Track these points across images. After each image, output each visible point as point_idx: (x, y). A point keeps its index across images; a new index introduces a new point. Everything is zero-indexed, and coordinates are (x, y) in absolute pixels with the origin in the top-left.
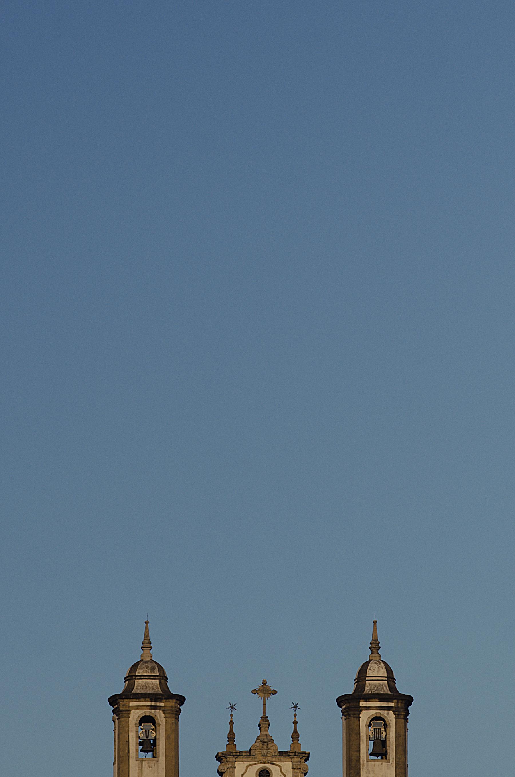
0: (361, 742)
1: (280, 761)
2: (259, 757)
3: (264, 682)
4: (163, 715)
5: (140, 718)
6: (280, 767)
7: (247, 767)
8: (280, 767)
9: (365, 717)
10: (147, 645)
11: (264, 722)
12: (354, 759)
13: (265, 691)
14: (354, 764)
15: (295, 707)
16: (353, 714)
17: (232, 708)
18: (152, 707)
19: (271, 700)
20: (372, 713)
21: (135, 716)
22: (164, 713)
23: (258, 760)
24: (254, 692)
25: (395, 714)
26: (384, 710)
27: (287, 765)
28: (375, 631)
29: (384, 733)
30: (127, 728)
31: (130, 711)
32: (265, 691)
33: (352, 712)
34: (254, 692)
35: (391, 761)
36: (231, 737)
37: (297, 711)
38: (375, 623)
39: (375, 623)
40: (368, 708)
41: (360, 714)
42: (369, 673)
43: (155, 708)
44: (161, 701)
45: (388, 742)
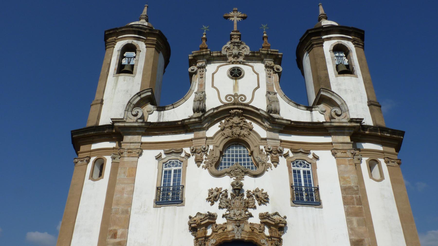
0: (327, 64)
2: (231, 59)
4: (145, 46)
5: (123, 46)
6: (252, 67)
7: (218, 67)
8: (252, 67)
9: (328, 46)
16: (316, 44)
20: (334, 42)
21: (119, 45)
22: (146, 44)
23: (229, 61)
25: (354, 44)
26: (345, 40)
27: (260, 67)
29: (347, 60)
30: (110, 55)
31: (116, 42)
33: (315, 43)
35: (359, 76)
41: (322, 43)
43: (138, 39)
45: (352, 66)
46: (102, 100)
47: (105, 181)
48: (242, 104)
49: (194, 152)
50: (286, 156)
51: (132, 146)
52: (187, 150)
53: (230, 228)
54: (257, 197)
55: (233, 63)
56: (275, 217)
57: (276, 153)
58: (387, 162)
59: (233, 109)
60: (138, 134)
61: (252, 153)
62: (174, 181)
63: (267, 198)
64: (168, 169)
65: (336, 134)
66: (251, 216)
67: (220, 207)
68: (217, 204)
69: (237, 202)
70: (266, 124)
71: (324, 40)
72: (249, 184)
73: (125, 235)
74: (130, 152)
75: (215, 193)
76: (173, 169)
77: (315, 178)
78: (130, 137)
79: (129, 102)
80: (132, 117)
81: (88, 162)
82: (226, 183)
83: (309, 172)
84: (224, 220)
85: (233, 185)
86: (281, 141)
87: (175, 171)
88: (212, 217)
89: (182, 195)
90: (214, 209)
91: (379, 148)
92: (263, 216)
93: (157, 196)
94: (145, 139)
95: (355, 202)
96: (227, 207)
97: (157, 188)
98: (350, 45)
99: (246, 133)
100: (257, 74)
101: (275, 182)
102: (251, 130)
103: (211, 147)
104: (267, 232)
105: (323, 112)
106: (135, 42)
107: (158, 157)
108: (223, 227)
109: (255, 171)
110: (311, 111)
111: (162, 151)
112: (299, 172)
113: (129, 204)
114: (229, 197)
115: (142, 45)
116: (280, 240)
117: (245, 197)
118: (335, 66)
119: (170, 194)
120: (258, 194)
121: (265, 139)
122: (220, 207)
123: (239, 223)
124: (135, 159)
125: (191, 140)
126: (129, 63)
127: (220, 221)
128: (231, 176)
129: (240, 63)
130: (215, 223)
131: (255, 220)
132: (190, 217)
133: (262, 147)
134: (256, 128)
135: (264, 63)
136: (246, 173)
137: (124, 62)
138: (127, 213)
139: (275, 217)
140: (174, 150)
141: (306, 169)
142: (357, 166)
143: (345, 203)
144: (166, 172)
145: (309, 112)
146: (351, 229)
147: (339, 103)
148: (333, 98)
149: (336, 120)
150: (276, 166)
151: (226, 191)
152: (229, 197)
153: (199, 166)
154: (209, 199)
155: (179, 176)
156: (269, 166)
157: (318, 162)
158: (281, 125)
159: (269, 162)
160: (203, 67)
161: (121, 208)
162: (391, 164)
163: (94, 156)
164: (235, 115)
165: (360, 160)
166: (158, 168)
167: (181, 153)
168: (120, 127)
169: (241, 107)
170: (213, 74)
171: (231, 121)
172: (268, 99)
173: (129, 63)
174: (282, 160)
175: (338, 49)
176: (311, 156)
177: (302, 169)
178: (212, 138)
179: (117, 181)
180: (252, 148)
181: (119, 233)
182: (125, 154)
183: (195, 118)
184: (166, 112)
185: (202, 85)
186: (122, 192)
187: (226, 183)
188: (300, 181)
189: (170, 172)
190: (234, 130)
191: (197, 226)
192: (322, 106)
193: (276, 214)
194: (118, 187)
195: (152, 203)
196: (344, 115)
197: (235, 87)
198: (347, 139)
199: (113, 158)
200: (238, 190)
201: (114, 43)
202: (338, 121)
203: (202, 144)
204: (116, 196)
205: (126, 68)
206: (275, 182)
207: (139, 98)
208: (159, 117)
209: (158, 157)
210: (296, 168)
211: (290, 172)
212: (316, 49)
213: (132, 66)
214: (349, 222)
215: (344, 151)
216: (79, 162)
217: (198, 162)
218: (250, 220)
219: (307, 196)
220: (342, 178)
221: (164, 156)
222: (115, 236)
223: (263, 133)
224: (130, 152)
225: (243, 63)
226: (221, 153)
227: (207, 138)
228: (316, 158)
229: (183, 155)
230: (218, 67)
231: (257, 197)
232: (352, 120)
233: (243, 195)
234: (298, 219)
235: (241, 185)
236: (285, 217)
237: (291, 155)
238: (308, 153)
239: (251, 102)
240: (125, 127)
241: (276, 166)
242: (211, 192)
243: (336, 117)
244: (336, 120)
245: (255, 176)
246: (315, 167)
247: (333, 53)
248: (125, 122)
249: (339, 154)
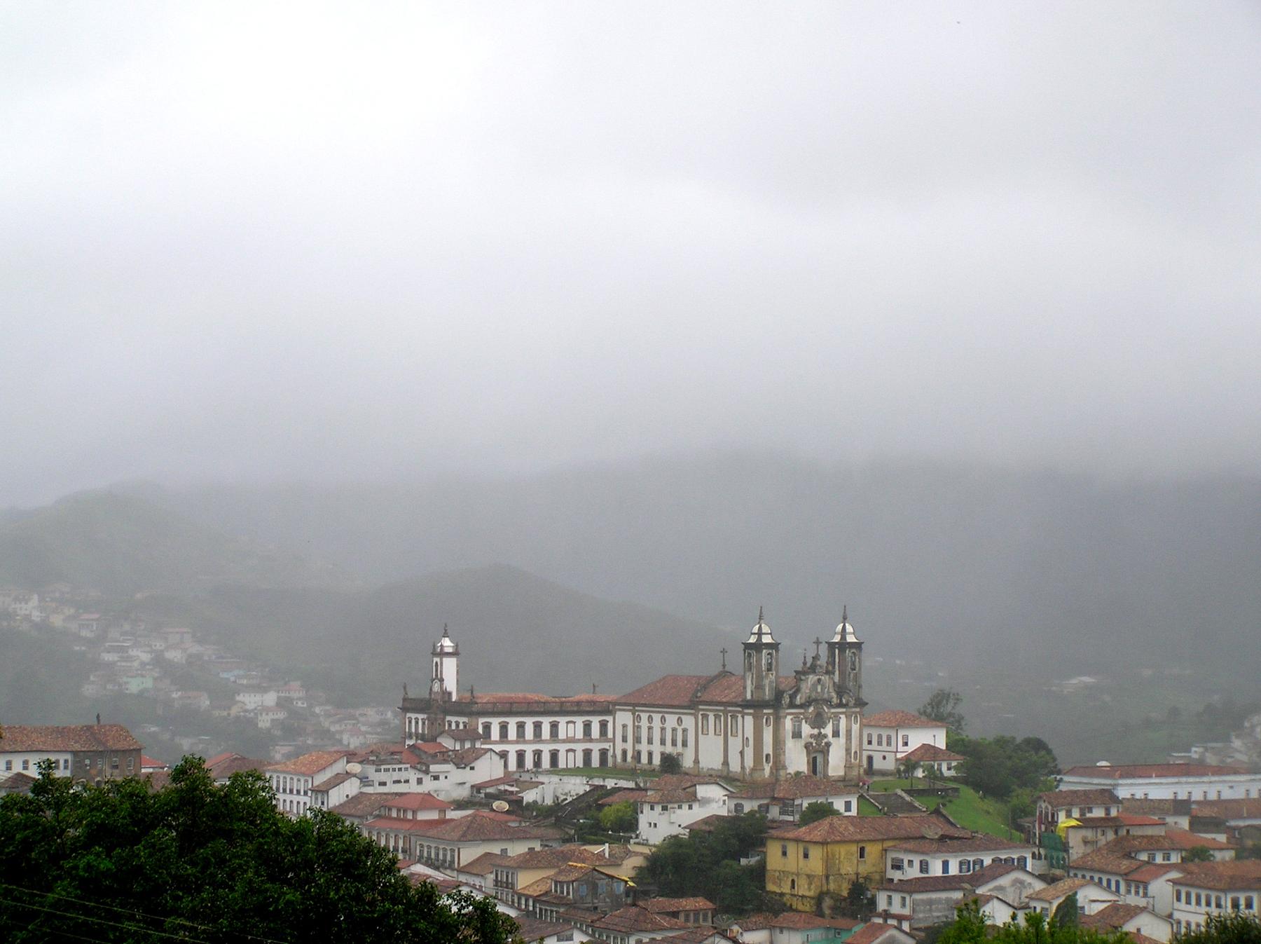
82: (816, 731)
101: (828, 730)
119: (797, 735)
140: (796, 716)
187: (816, 731)
191: (807, 746)
206: (828, 730)
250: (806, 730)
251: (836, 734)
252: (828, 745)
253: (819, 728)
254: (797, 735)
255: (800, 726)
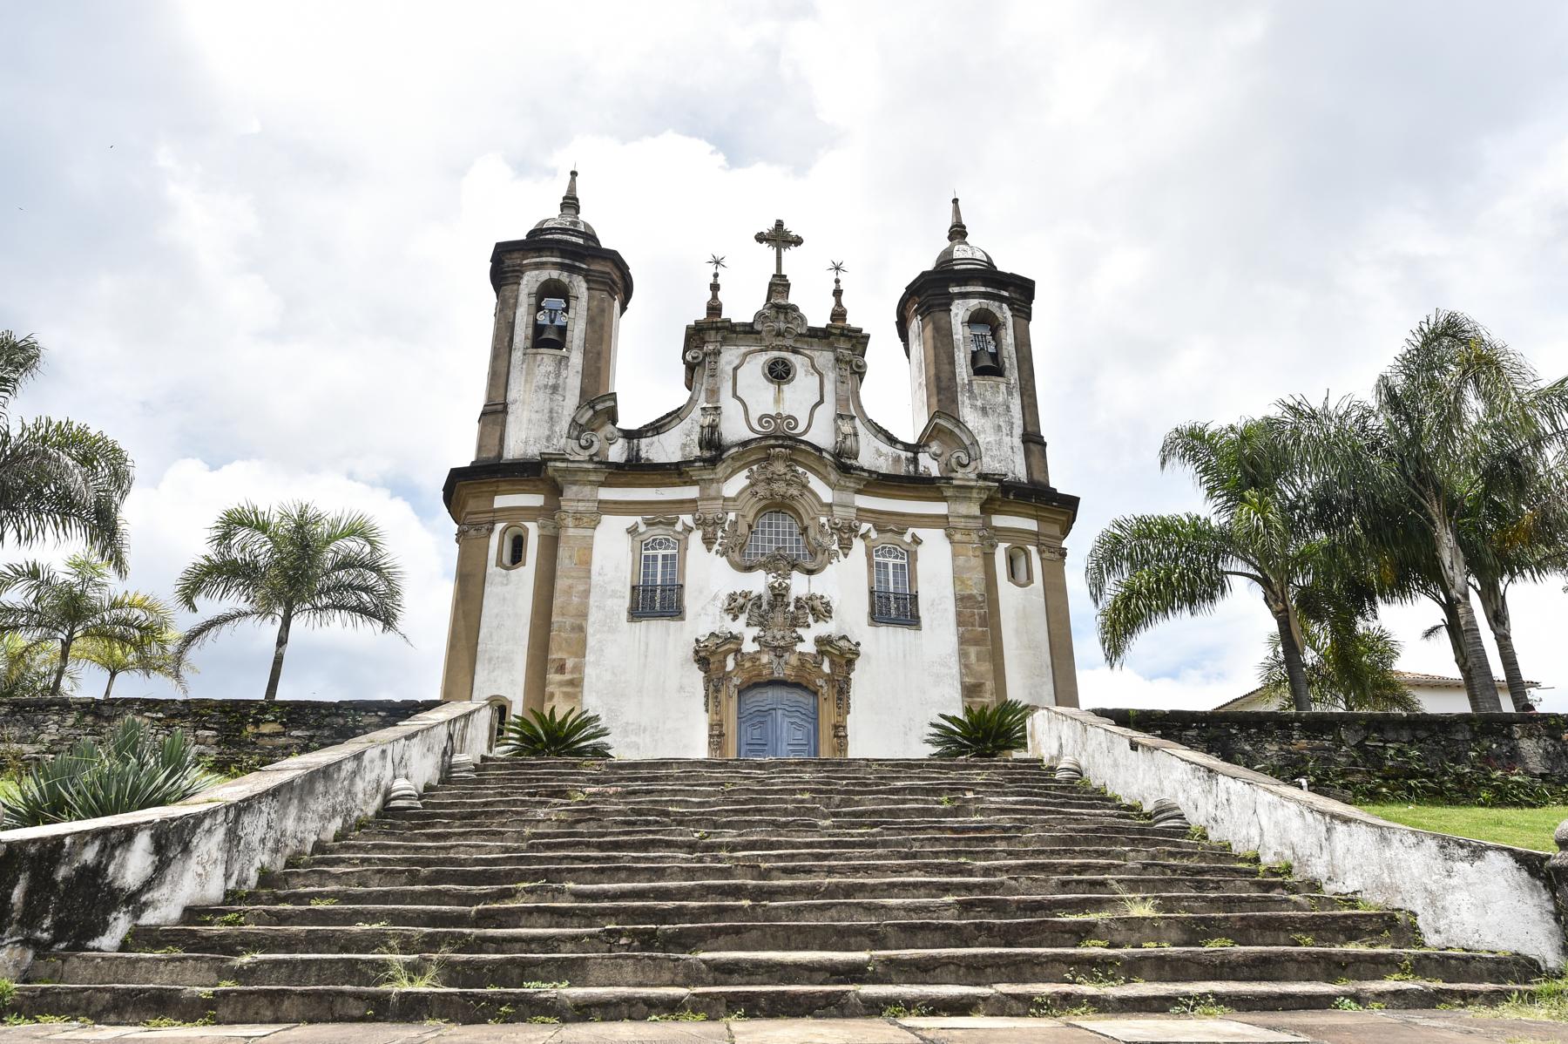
1: (811, 346)
3: (779, 224)
4: (584, 285)
6: (811, 358)
7: (746, 355)
8: (811, 358)
9: (960, 311)
10: (570, 203)
11: (779, 284)
12: (945, 376)
13: (780, 238)
14: (943, 385)
15: (837, 269)
17: (718, 263)
18: (562, 267)
19: (789, 254)
20: (974, 303)
22: (587, 281)
24: (760, 238)
27: (824, 358)
28: (957, 211)
32: (780, 238)
34: (760, 238)
36: (714, 308)
37: (841, 276)
38: (955, 201)
39: (955, 201)
40: (965, 296)
42: (956, 255)
44: (582, 259)
46: (505, 405)
47: (527, 572)
48: (791, 438)
49: (701, 523)
50: (864, 537)
51: (581, 506)
52: (687, 519)
53: (765, 659)
54: (813, 609)
55: (773, 349)
56: (842, 643)
57: (846, 534)
58: (1040, 552)
59: (774, 447)
60: (591, 483)
61: (805, 530)
62: (664, 574)
63: (829, 612)
64: (651, 552)
65: (956, 499)
66: (801, 639)
67: (748, 625)
68: (743, 618)
69: (779, 617)
70: (833, 476)
71: (951, 298)
72: (799, 585)
73: (579, 668)
74: (578, 517)
75: (741, 601)
76: (660, 553)
77: (913, 578)
78: (575, 488)
79: (574, 420)
80: (581, 452)
81: (491, 530)
82: (758, 583)
83: (903, 566)
84: (756, 647)
85: (772, 588)
86: (859, 509)
87: (665, 557)
88: (735, 639)
89: (680, 600)
90: (738, 626)
91: (1031, 525)
92: (820, 641)
93: (634, 600)
94: (606, 494)
95: (979, 621)
96: (761, 624)
97: (633, 588)
98: (1005, 314)
99: (796, 493)
100: (821, 375)
101: (843, 583)
102: (805, 486)
103: (732, 516)
104: (826, 667)
105: (935, 457)
106: (564, 277)
107: (632, 531)
108: (754, 658)
109: (810, 566)
110: (916, 453)
111: (639, 519)
112: (886, 565)
113: (584, 615)
114: (765, 606)
115: (580, 286)
116: (847, 681)
117: (792, 608)
118: (969, 356)
120: (817, 603)
121: (830, 505)
122: (748, 625)
123: (780, 651)
124: (588, 532)
125: (694, 501)
126: (552, 321)
127: (749, 647)
128: (769, 571)
129: (787, 349)
130: (738, 651)
131: (808, 647)
132: (697, 641)
133: (823, 520)
134: (815, 483)
135: (834, 350)
136: (794, 566)
137: (542, 318)
138: (581, 629)
139: (842, 643)
140: (659, 515)
141: (898, 561)
142: (989, 559)
143: (960, 622)
144: (647, 557)
145: (910, 455)
146: (965, 666)
147: (967, 442)
148: (957, 431)
149: (959, 475)
150: (846, 555)
151: (760, 597)
152: (765, 606)
153: (709, 550)
154: (728, 610)
155: (673, 566)
156: (836, 554)
157: (920, 549)
158: (861, 479)
159: (835, 547)
160: (717, 353)
161: (569, 621)
162: (1046, 555)
163: (501, 521)
164: (777, 457)
165: (994, 546)
166: (633, 551)
167: (673, 524)
168: (557, 470)
169: (789, 443)
170: (735, 369)
171: (771, 468)
172: (837, 429)
173: (552, 321)
174: (859, 546)
175: (979, 319)
176: (907, 538)
177: (891, 561)
178: (734, 499)
179: (558, 573)
180: (806, 522)
181: (569, 664)
182: (570, 521)
183: (704, 460)
184: (643, 441)
185: (713, 393)
186: (569, 591)
187: (758, 583)
188: (887, 581)
189: (655, 558)
190: (775, 486)
191: (705, 658)
192: (935, 447)
193: (844, 637)
194: (561, 584)
195: (624, 615)
196: (973, 464)
197: (777, 401)
198: (978, 513)
199: (541, 527)
200: (779, 595)
201: (518, 273)
202: (960, 476)
203: (711, 509)
204: (558, 602)
205: (551, 335)
206: (843, 583)
207: (591, 412)
208: (630, 449)
209: (632, 531)
210: (880, 559)
211: (870, 566)
212: (940, 315)
213: (562, 330)
214: (963, 655)
215: (967, 531)
216: (472, 532)
217: (708, 542)
218: (800, 647)
219: (897, 609)
220: (957, 577)
221: (642, 528)
222: (561, 669)
223: (826, 494)
224: (578, 517)
225: (795, 351)
226: (750, 527)
227: (725, 499)
228: (917, 541)
229: (679, 527)
230: (746, 355)
231: (813, 609)
232: (983, 476)
233: (788, 605)
234: (880, 648)
235: (787, 588)
236: (858, 644)
237: (873, 535)
238: (902, 533)
239: (806, 432)
240: (567, 469)
241: (846, 555)
242: (733, 597)
243: (960, 470)
244: (959, 475)
245: (810, 572)
246: (913, 557)
247: (967, 330)
248: (568, 460)
249: (958, 537)
250: (710, 579)
251: (895, 608)
252: (842, 656)
253: (781, 563)
254: (656, 600)
255: (674, 564)
